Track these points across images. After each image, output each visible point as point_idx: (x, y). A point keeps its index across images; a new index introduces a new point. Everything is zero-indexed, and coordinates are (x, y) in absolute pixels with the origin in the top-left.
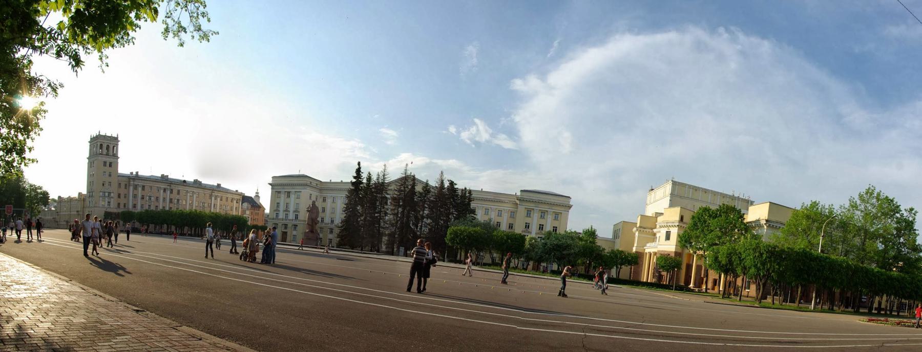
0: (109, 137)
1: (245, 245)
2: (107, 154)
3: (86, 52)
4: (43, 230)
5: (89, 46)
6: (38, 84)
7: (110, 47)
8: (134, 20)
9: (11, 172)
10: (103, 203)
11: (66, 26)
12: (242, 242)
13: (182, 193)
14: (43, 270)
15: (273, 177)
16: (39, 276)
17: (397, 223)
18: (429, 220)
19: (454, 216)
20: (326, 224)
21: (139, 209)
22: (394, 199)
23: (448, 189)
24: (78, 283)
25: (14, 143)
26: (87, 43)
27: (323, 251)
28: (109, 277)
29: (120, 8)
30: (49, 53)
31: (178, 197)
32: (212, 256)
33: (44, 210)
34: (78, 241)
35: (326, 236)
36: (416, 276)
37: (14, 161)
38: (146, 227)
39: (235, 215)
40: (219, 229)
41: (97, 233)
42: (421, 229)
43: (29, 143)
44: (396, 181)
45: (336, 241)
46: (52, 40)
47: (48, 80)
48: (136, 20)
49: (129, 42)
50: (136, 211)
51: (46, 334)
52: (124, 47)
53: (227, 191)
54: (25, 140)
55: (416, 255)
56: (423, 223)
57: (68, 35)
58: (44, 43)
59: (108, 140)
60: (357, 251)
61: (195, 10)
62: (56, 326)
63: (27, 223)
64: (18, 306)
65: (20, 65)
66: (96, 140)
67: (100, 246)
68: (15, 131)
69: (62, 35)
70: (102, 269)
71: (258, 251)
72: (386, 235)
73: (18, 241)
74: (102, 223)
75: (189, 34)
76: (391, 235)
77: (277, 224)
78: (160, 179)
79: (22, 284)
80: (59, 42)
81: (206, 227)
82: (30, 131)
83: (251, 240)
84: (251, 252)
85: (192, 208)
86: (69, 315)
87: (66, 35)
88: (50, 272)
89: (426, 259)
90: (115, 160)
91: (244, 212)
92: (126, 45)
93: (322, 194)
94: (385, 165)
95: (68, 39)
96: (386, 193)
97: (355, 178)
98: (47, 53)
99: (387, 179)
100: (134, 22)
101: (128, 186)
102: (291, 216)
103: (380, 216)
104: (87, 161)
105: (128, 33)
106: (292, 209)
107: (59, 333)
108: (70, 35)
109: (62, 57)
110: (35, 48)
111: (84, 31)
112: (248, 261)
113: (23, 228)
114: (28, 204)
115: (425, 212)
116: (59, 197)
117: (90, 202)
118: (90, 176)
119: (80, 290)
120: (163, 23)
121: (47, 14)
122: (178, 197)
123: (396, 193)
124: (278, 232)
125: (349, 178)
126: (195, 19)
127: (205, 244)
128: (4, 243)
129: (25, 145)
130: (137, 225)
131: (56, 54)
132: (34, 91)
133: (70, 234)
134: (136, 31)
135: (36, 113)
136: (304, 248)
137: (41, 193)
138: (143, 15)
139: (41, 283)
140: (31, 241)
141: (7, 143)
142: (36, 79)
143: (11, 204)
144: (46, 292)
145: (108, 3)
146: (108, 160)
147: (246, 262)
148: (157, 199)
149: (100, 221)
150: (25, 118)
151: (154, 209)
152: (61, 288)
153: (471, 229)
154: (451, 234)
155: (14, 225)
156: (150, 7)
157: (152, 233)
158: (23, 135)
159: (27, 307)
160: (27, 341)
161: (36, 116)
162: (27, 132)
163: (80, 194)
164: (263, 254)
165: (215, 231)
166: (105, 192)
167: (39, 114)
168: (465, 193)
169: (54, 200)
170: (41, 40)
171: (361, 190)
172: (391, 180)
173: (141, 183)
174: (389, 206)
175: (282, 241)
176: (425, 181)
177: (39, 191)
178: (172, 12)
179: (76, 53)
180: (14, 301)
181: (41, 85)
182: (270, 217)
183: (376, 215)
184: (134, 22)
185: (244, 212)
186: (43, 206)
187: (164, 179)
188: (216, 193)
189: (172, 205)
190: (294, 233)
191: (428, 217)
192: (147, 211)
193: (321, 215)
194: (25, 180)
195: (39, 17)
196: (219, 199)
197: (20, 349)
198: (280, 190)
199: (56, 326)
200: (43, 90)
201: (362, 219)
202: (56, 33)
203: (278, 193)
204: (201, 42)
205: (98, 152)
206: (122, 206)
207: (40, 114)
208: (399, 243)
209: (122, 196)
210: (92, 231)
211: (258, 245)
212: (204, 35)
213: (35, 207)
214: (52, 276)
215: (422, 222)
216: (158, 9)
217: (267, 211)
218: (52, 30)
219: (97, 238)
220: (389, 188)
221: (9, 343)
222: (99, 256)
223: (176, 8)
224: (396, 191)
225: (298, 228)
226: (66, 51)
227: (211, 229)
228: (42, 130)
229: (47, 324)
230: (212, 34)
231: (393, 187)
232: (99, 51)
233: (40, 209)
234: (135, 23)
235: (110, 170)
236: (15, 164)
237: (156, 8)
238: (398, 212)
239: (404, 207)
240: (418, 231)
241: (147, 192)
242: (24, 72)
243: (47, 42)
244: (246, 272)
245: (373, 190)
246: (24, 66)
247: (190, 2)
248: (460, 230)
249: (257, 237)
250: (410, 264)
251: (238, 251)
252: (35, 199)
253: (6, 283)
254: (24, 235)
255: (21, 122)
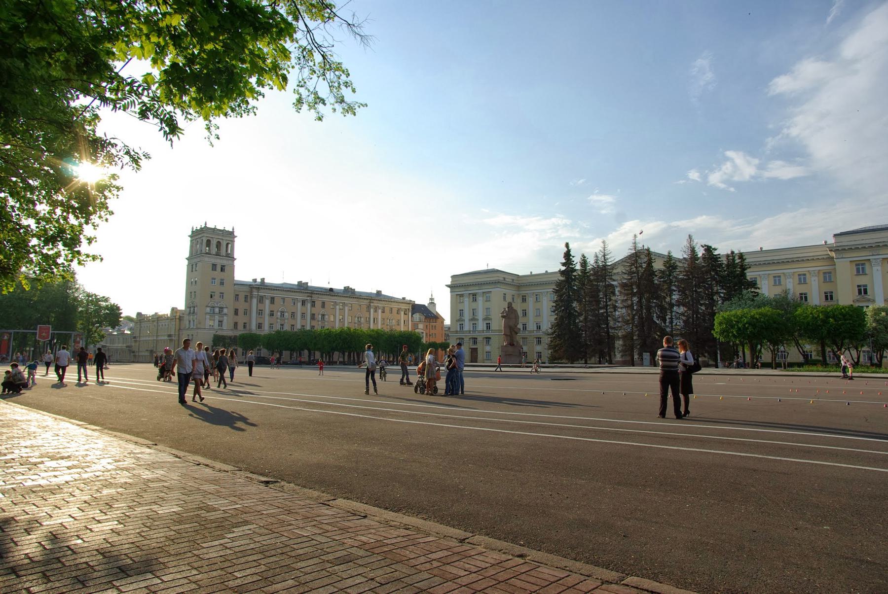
0: (220, 230)
1: (421, 372)
2: (218, 254)
3: (186, 117)
4: (108, 366)
5: (191, 111)
6: (108, 149)
7: (221, 115)
8: (255, 86)
9: (53, 273)
10: (211, 323)
11: (157, 80)
12: (416, 368)
13: (329, 305)
14: (106, 431)
15: (453, 277)
16: (96, 441)
17: (633, 318)
18: (682, 307)
19: (720, 297)
20: (530, 332)
21: (266, 330)
22: (623, 286)
23: (704, 258)
24: (168, 448)
25: (60, 229)
26: (188, 106)
27: (530, 370)
28: (221, 434)
29: (235, 71)
30: (128, 110)
31: (322, 311)
32: (376, 390)
33: (111, 334)
34: (170, 381)
35: (532, 349)
36: (670, 394)
37: (58, 255)
38: (278, 356)
39: (404, 332)
40: (382, 352)
41: (201, 368)
42: (671, 322)
43: (88, 230)
44: (622, 261)
45: (547, 353)
46: (133, 94)
47: (125, 146)
48: (258, 86)
49: (248, 112)
50: (262, 334)
51: (107, 542)
52: (241, 117)
53: (390, 300)
54: (81, 225)
55: (662, 361)
56: (674, 314)
57: (159, 91)
58: (120, 96)
59: (219, 235)
60: (580, 365)
61: (335, 79)
62: (126, 524)
63: (79, 355)
64: (52, 499)
65: (78, 117)
66: (200, 234)
67: (206, 387)
68: (63, 211)
69: (150, 91)
70: (208, 422)
71: (439, 379)
72: (620, 338)
73: (61, 384)
74: (210, 352)
75: (329, 107)
76: (628, 337)
77: (463, 339)
78: (296, 287)
79: (62, 458)
80: (145, 99)
81: (364, 351)
82: (91, 214)
83: (429, 364)
84: (430, 380)
85: (344, 325)
86: (150, 504)
87: (155, 92)
88: (118, 434)
89: (684, 365)
90: (230, 262)
91: (415, 325)
92: (244, 115)
93: (521, 292)
94: (604, 242)
95: (158, 98)
96: (611, 279)
97: (564, 264)
98: (124, 110)
99: (609, 260)
100: (254, 88)
101: (249, 299)
102: (481, 326)
103: (607, 312)
104: (186, 262)
105: (247, 101)
106: (480, 315)
107: (132, 536)
108: (161, 93)
109: (148, 118)
110: (104, 100)
111: (184, 92)
112: (427, 394)
113: (70, 363)
114: (82, 324)
115: (673, 297)
116: (139, 314)
117: (190, 321)
118: (190, 283)
119: (171, 459)
120: (294, 92)
121: (127, 60)
122: (322, 311)
123: (626, 276)
124: (465, 350)
125: (556, 266)
126: (336, 89)
127: (365, 374)
128: (30, 389)
129: (80, 234)
130: (264, 353)
131: (139, 114)
132: (101, 158)
133: (156, 371)
134: (258, 100)
135: (102, 188)
136: (503, 369)
137: (107, 308)
138: (267, 80)
139: (101, 453)
140: (85, 384)
141: (47, 227)
142: (105, 142)
143: (48, 323)
144: (109, 467)
145: (218, 63)
146: (219, 262)
147: (423, 395)
148: (293, 315)
149: (207, 349)
150: (83, 194)
151: (290, 330)
152: (138, 459)
153: (754, 312)
154: (720, 324)
155: (52, 358)
156: (277, 73)
157: (287, 364)
158: (78, 218)
159: (72, 499)
160: (68, 561)
161: (103, 193)
162: (85, 213)
163: (174, 310)
164: (447, 382)
165: (377, 355)
166: (214, 307)
167: (107, 191)
168: (734, 260)
169: (129, 319)
170: (116, 91)
171: (574, 280)
172: (615, 261)
173: (269, 294)
174: (619, 297)
175: (471, 362)
176: (666, 254)
177: (103, 304)
178: (306, 81)
179: (172, 117)
180: (46, 491)
181: (113, 151)
182: (451, 330)
183: (601, 311)
184: (254, 88)
185: (415, 325)
186: (110, 328)
187: (302, 287)
188: (375, 304)
189: (314, 323)
190: (488, 348)
191: (679, 303)
192: (278, 332)
193: (522, 320)
194: (77, 286)
195: (113, 61)
196: (380, 311)
197: (52, 578)
198: (462, 293)
199: (126, 524)
200: (116, 159)
201: (581, 319)
202: (140, 86)
203: (460, 297)
204: (345, 116)
205: (204, 251)
206: (240, 327)
207: (110, 191)
208: (641, 347)
209: (241, 312)
210: (193, 365)
211: (439, 369)
212: (349, 107)
213: (94, 329)
214: (121, 439)
215: (671, 312)
216: (287, 76)
217: (447, 322)
218: (134, 82)
219: (200, 374)
220: (615, 271)
221: (29, 572)
222: (203, 401)
223: (311, 76)
224: (625, 274)
225: (491, 341)
226: (156, 112)
227: (371, 353)
228: (113, 213)
229: (110, 523)
230: (359, 107)
231: (620, 269)
232: (206, 118)
233: (103, 332)
234: (256, 90)
235: (223, 275)
236: (60, 261)
237: (285, 75)
238: (632, 304)
239: (640, 295)
240: (668, 326)
241: (278, 307)
242: (85, 130)
243: (125, 95)
244: (424, 410)
245: (592, 278)
246: (85, 121)
247: (328, 71)
248: (735, 316)
249: (436, 359)
250: (658, 377)
251: (411, 381)
252: (95, 317)
253: (29, 459)
254: (71, 375)
255: (74, 199)
